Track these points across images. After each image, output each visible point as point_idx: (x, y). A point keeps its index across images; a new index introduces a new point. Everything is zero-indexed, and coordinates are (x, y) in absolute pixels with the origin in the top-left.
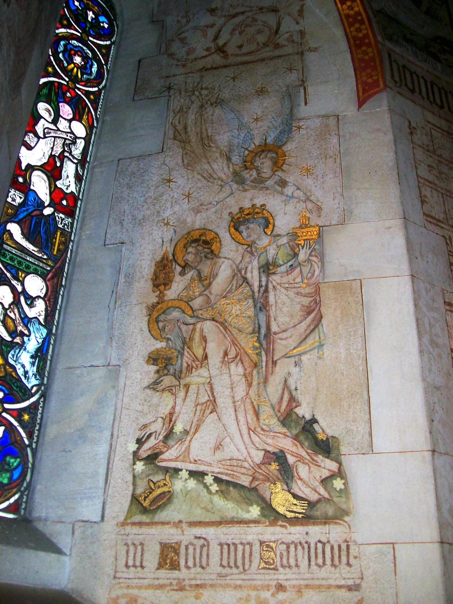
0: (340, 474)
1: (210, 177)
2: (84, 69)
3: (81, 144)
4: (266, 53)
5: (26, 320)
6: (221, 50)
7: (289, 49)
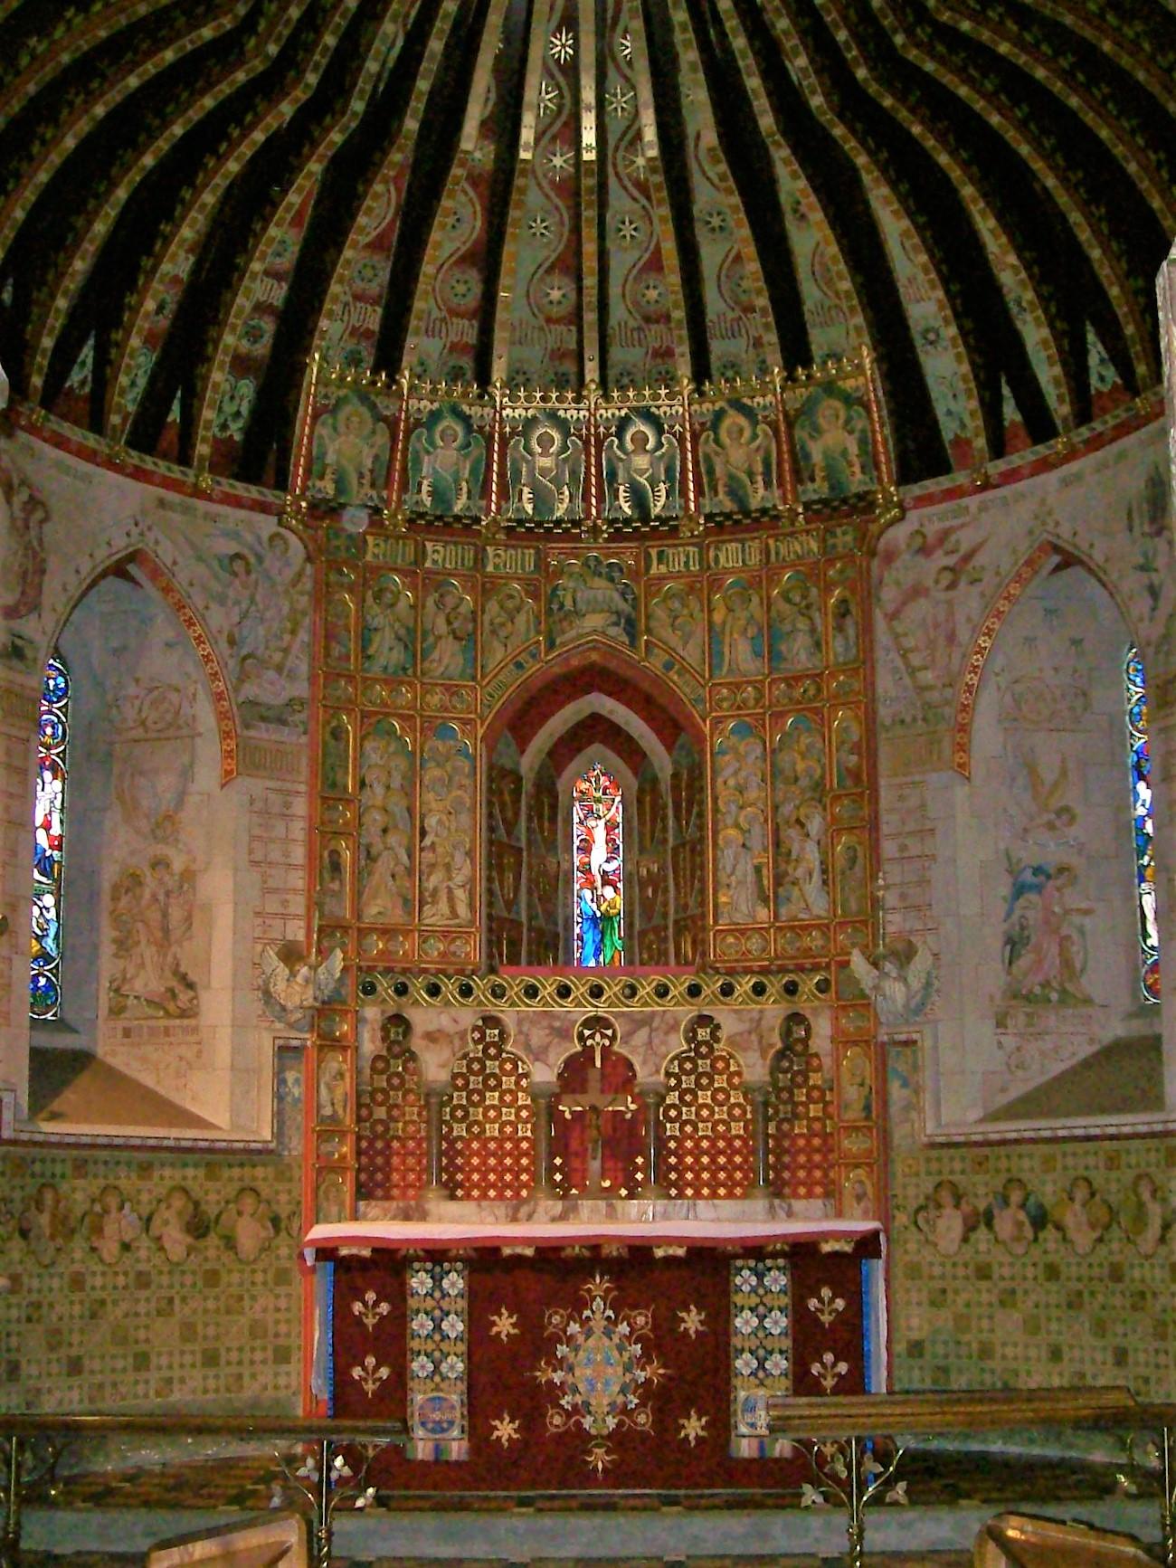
0: (196, 997)
1: (138, 832)
2: (54, 735)
3: (60, 796)
4: (171, 733)
5: (47, 921)
6: (143, 723)
7: (185, 731)
